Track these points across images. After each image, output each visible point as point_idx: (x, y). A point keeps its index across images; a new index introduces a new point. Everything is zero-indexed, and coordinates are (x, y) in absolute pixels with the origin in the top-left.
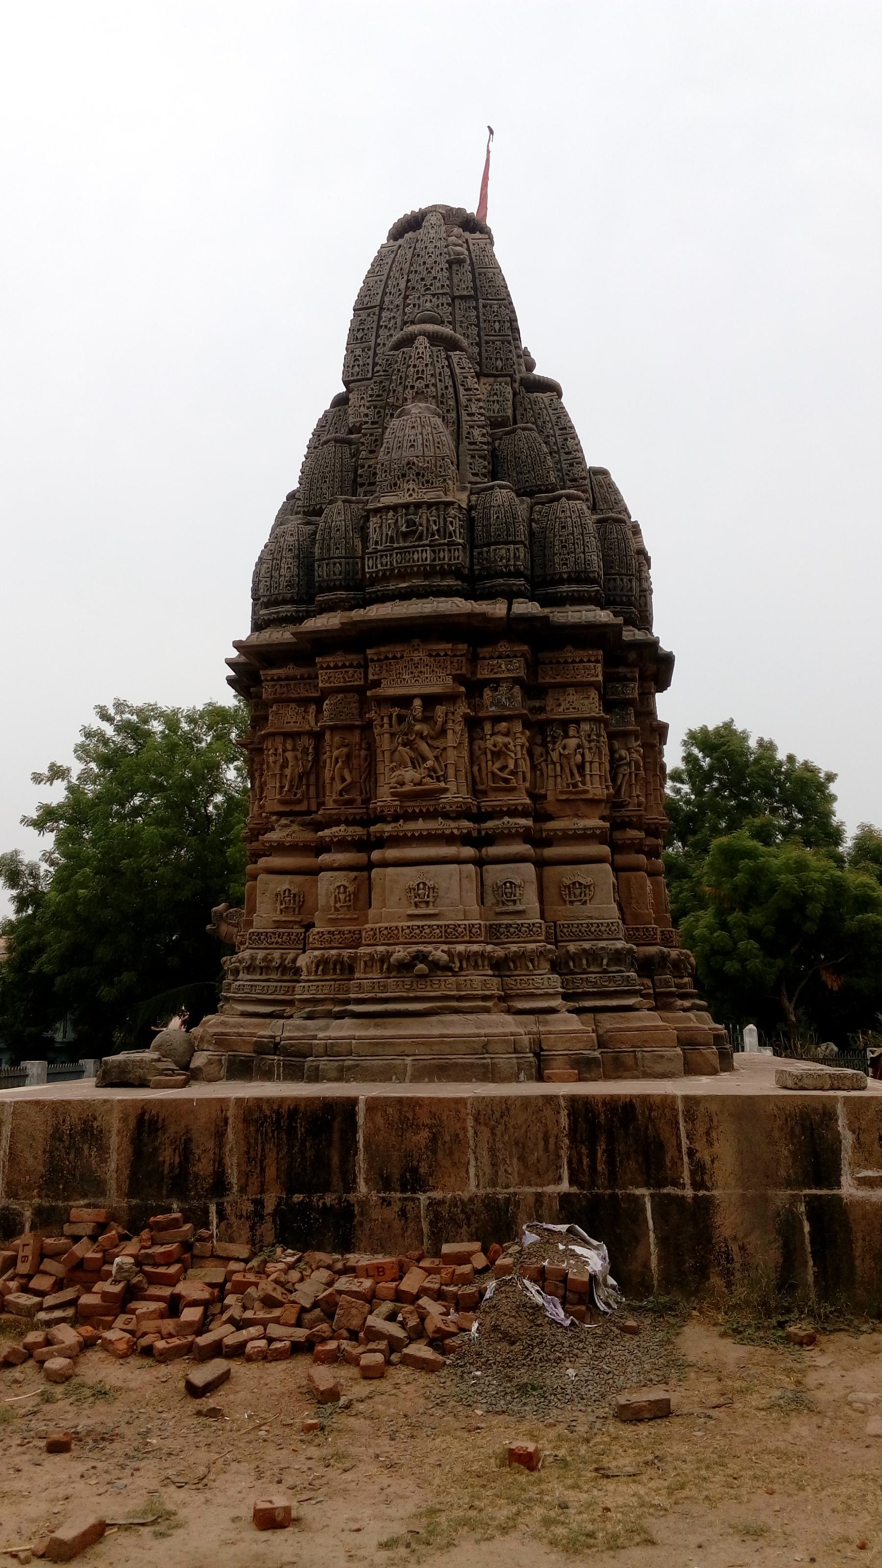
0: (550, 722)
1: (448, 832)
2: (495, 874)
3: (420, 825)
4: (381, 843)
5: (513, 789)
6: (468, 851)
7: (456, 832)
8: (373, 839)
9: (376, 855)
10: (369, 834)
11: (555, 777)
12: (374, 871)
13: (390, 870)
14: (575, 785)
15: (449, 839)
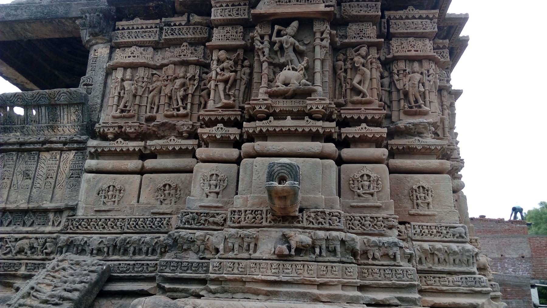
0: (396, 59)
1: (314, 130)
2: (353, 170)
3: (289, 122)
4: (251, 139)
5: (370, 103)
6: (330, 147)
7: (321, 131)
8: (245, 137)
9: (246, 146)
10: (241, 135)
11: (399, 101)
12: (245, 161)
13: (258, 159)
14: (420, 107)
15: (314, 136)
